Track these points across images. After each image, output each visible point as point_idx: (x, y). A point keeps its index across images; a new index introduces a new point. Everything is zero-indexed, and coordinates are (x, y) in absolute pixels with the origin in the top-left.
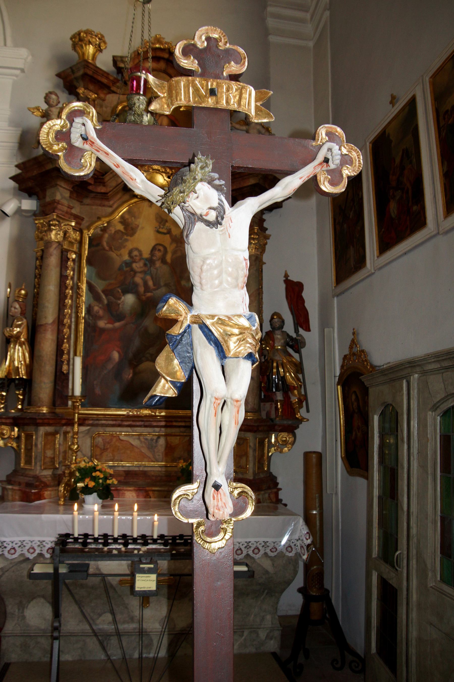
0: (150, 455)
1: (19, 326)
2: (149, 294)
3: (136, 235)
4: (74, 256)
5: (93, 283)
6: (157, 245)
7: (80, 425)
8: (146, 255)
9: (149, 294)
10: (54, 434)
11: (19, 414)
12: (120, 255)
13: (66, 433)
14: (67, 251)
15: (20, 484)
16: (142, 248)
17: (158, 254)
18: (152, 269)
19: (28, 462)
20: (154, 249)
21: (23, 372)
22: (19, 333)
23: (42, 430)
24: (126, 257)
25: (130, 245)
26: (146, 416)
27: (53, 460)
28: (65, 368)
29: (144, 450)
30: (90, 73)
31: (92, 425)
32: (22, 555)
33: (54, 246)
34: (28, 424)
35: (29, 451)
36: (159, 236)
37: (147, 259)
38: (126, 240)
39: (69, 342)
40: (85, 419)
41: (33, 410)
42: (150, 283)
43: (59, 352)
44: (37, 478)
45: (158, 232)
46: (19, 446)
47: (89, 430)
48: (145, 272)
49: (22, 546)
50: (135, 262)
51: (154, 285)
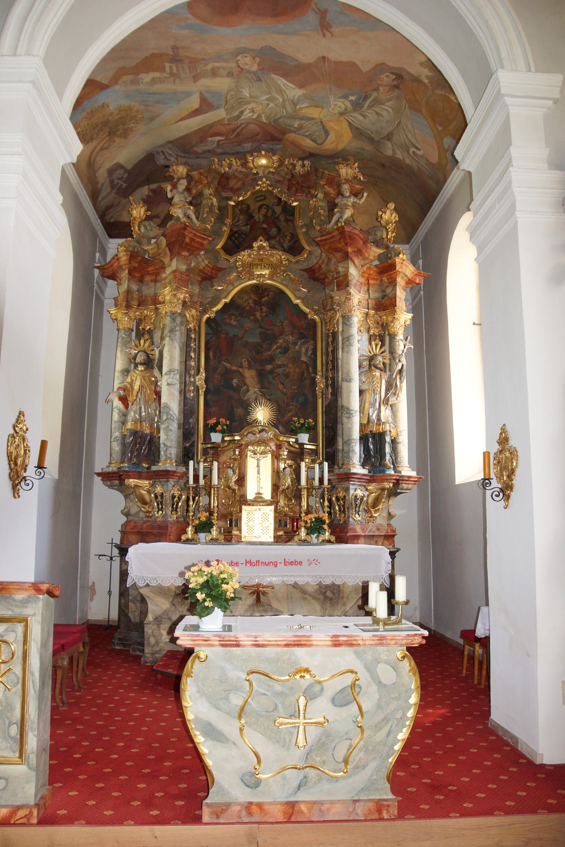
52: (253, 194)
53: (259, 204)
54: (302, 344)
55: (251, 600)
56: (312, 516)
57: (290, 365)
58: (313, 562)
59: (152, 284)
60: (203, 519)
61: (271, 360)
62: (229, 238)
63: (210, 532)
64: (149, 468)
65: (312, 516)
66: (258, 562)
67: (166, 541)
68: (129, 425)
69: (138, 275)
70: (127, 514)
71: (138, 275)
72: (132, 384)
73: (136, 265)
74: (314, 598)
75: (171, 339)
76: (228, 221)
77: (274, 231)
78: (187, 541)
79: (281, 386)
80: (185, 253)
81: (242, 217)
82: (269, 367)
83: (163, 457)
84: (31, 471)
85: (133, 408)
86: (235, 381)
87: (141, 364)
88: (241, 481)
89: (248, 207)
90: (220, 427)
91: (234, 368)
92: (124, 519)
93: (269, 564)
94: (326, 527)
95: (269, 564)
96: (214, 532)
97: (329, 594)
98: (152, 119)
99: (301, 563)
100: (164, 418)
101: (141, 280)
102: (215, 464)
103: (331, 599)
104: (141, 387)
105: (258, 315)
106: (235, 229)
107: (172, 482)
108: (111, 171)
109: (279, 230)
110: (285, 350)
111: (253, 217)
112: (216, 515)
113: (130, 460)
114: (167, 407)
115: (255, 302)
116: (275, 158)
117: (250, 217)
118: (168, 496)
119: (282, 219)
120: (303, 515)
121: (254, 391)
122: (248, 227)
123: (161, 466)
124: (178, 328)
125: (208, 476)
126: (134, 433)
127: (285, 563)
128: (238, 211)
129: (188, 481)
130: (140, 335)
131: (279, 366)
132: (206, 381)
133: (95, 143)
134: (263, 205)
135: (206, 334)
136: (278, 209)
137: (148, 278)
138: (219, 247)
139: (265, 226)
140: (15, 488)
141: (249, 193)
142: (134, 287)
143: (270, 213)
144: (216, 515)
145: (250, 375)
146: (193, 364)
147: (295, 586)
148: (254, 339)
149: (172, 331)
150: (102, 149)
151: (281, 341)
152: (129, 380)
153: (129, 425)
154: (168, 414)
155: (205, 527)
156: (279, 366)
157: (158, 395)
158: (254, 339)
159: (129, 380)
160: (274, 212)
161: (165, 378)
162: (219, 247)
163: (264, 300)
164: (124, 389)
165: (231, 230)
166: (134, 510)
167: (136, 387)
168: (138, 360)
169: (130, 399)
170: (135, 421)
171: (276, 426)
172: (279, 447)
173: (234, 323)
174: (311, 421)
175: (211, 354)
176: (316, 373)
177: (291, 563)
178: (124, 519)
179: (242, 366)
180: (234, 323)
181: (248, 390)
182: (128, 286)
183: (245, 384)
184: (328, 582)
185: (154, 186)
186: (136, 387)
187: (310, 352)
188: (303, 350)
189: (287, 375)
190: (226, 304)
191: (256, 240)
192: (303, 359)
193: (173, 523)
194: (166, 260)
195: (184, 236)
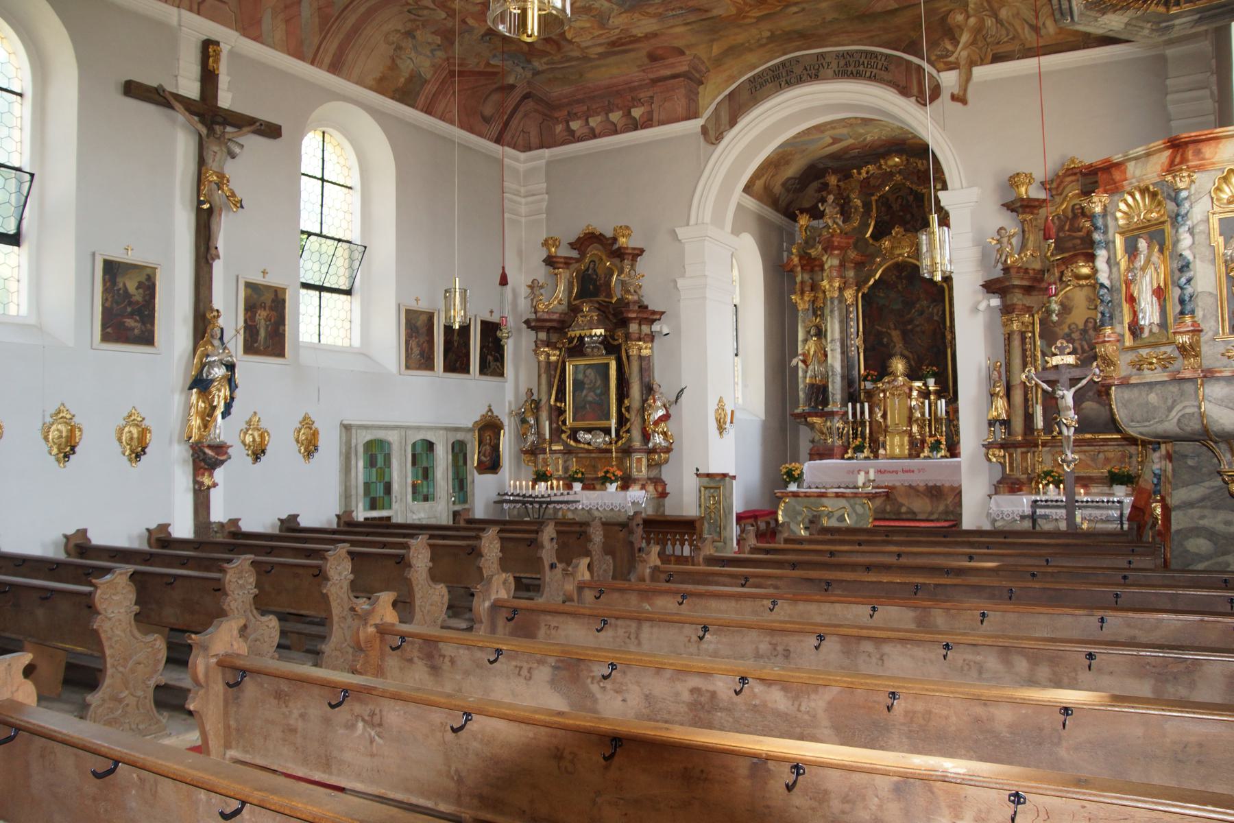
0: (1093, 465)
1: (999, 386)
2: (1085, 355)
3: (1073, 313)
4: (1030, 335)
5: (1045, 350)
6: (1088, 318)
7: (1043, 446)
8: (1081, 326)
9: (1085, 355)
10: (1027, 452)
11: (1003, 442)
12: (1063, 329)
13: (1034, 452)
14: (1025, 332)
15: (1007, 483)
16: (1077, 322)
17: (1090, 325)
18: (1086, 336)
19: (1012, 469)
20: (1087, 321)
21: (1004, 416)
22: (999, 391)
23: (1019, 450)
24: (1067, 330)
25: (1069, 321)
26: (1089, 439)
27: (1027, 469)
28: (1030, 410)
29: (1089, 462)
30: (1025, 203)
31: (1052, 446)
32: (1013, 518)
33: (1016, 333)
34: (1010, 447)
35: (1011, 464)
36: (1089, 311)
37: (1082, 330)
38: (1066, 318)
39: (1032, 393)
40: (1046, 443)
41: (1012, 438)
42: (1086, 347)
43: (1026, 400)
44: (1018, 479)
45: (1089, 309)
46: (1005, 462)
47: (1050, 451)
48: (1081, 339)
49: (1013, 513)
50: (1073, 332)
51: (1089, 347)
52: (890, 188)
53: (895, 196)
54: (934, 306)
55: (883, 498)
56: (932, 440)
57: (926, 325)
58: (921, 470)
59: (820, 273)
60: (858, 443)
61: (911, 321)
62: (875, 227)
63: (863, 452)
64: (823, 409)
65: (932, 440)
66: (885, 471)
67: (833, 458)
68: (808, 380)
69: (808, 268)
70: (813, 441)
71: (808, 268)
72: (809, 351)
73: (805, 262)
74: (924, 495)
75: (832, 317)
76: (874, 214)
77: (908, 216)
78: (849, 459)
79: (919, 341)
80: (836, 252)
81: (883, 209)
82: (910, 327)
83: (831, 402)
84: (728, 425)
85: (811, 367)
86: (885, 340)
87: (815, 336)
88: (884, 416)
89: (888, 199)
90: (869, 378)
91: (884, 330)
92: (811, 445)
93: (893, 472)
94: (942, 446)
95: (893, 472)
96: (866, 452)
97: (934, 492)
98: (804, 151)
99: (913, 471)
100: (830, 374)
101: (812, 270)
102: (866, 405)
103: (936, 496)
104: (815, 352)
105: (900, 287)
106: (879, 220)
107: (837, 418)
108: (784, 185)
109: (913, 215)
110: (922, 313)
111: (891, 207)
112: (867, 440)
113: (810, 405)
114: (832, 366)
115: (897, 277)
116: (904, 157)
117: (890, 207)
118: (834, 429)
119: (915, 206)
120: (927, 438)
121: (899, 346)
122: (889, 216)
123: (830, 408)
124: (836, 309)
125: (862, 413)
126: (812, 386)
127: (904, 471)
128: (880, 204)
129: (848, 418)
130: (815, 314)
131: (918, 326)
132: (865, 341)
133: (766, 176)
134: (898, 197)
135: (862, 306)
136: (911, 198)
137: (817, 269)
138: (868, 235)
139: (901, 214)
140: (721, 433)
141: (887, 188)
142: (806, 277)
143: (904, 202)
144: (867, 440)
145: (896, 335)
146: (852, 330)
147: (910, 487)
148: (897, 306)
149: (832, 311)
150: (772, 176)
151: (918, 306)
152: (807, 348)
153: (808, 380)
154: (833, 371)
155: (859, 449)
156: (918, 326)
157: (826, 356)
158: (897, 306)
159: (807, 348)
160: (908, 201)
161: (829, 345)
162: (868, 235)
163: (903, 274)
164: (804, 355)
165: (876, 221)
166: (817, 438)
167: (812, 353)
168: (812, 333)
169: (808, 363)
170: (811, 377)
171: (907, 376)
172: (911, 389)
173: (882, 295)
174: (935, 368)
175: (867, 320)
176: (945, 328)
177: (907, 471)
178: (811, 445)
179: (889, 328)
180: (882, 295)
181: (895, 346)
182: (802, 278)
183: (892, 341)
184: (931, 484)
185: (822, 181)
186: (812, 353)
187: (940, 313)
188: (935, 311)
189: (923, 332)
190: (875, 281)
191: (894, 228)
192: (936, 318)
193: (838, 447)
194: (824, 258)
195: (833, 242)
